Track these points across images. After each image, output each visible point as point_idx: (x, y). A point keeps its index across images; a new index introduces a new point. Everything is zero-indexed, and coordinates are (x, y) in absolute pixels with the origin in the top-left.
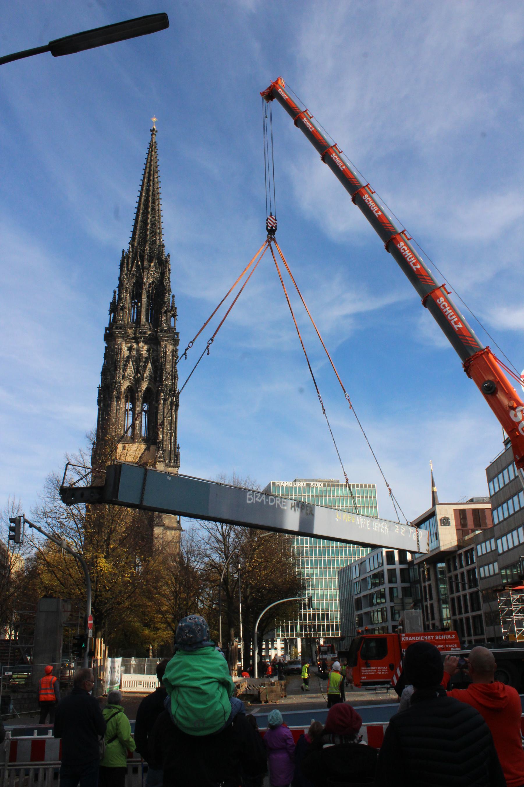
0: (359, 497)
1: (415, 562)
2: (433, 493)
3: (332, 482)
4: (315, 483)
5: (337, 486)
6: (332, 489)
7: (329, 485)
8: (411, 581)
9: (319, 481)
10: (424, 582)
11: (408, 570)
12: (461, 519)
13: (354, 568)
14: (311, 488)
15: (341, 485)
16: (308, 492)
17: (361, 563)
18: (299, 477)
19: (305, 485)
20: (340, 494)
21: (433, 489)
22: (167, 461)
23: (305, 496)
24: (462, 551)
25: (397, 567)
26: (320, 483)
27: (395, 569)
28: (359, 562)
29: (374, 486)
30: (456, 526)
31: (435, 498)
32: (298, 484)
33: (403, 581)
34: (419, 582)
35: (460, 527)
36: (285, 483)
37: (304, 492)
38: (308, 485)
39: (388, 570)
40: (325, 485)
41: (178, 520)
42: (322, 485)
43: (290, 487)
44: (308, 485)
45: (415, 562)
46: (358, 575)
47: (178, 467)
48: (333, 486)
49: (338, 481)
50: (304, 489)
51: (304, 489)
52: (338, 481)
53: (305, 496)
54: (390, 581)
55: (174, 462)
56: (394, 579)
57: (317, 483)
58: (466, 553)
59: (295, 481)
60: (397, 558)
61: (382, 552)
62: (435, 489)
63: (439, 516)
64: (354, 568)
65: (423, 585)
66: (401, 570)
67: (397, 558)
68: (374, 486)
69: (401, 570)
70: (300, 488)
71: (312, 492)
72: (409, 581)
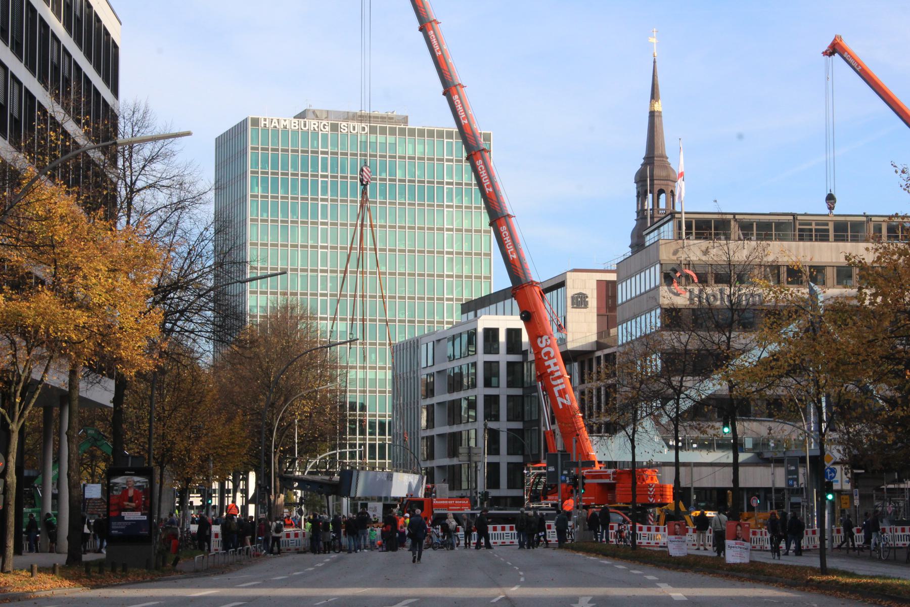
0: (451, 161)
2: (652, 115)
4: (351, 124)
5: (402, 132)
6: (390, 139)
7: (383, 131)
8: (526, 385)
11: (522, 363)
12: (608, 297)
13: (424, 347)
15: (412, 132)
16: (335, 144)
17: (439, 341)
18: (316, 107)
19: (328, 128)
20: (409, 153)
21: (652, 105)
23: (327, 153)
24: (598, 354)
25: (503, 357)
27: (498, 362)
28: (435, 338)
30: (598, 309)
31: (657, 129)
32: (312, 124)
33: (510, 385)
35: (604, 311)
36: (282, 122)
37: (325, 145)
39: (485, 362)
40: (373, 130)
42: (367, 130)
43: (293, 131)
44: (335, 127)
46: (430, 363)
48: (393, 132)
49: (405, 120)
50: (325, 137)
51: (325, 137)
52: (405, 120)
53: (327, 153)
54: (488, 384)
56: (494, 380)
58: (607, 356)
62: (658, 107)
63: (571, 289)
64: (424, 347)
66: (510, 364)
69: (510, 364)
70: (315, 133)
71: (343, 144)
72: (522, 387)
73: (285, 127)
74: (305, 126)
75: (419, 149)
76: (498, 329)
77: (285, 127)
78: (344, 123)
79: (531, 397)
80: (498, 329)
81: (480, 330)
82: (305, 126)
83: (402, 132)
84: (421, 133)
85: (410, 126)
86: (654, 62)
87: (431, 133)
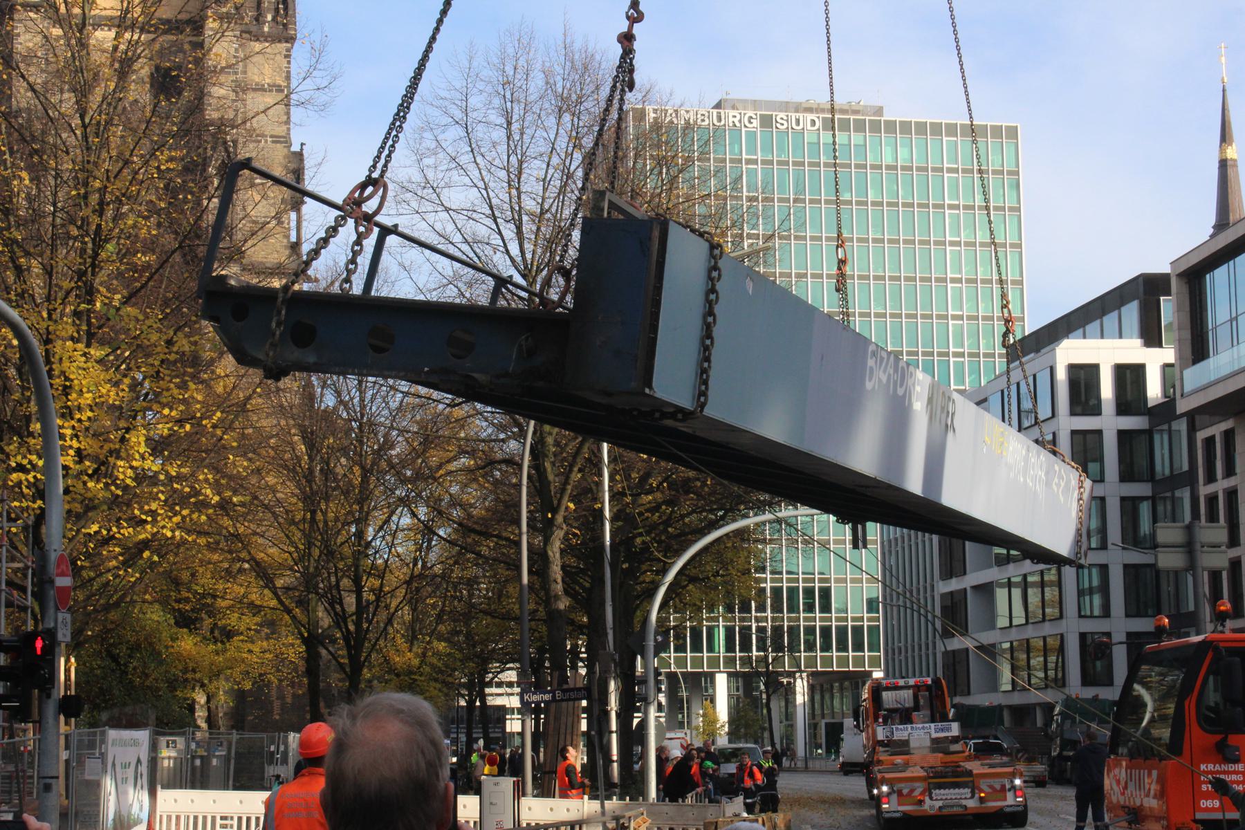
0: (956, 171)
1: (1182, 407)
2: (1224, 164)
3: (856, 112)
4: (794, 116)
5: (875, 127)
6: (856, 138)
8: (1158, 477)
9: (809, 110)
10: (1211, 478)
11: (1149, 433)
14: (779, 132)
15: (890, 126)
16: (768, 148)
18: (734, 95)
19: (756, 123)
20: (888, 159)
21: (1222, 150)
22: (250, 14)
23: (755, 162)
25: (1109, 423)
26: (810, 116)
29: (1013, 132)
33: (1127, 475)
34: (1189, 479)
37: (752, 149)
38: (767, 121)
39: (1073, 432)
41: (293, 239)
42: (818, 124)
44: (767, 121)
45: (1182, 407)
47: (291, 39)
48: (860, 127)
49: (879, 111)
50: (752, 136)
51: (752, 136)
52: (879, 111)
55: (274, 19)
57: (801, 115)
59: (718, 106)
60: (1107, 390)
61: (1052, 370)
62: (1231, 153)
65: (1204, 490)
66: (1123, 435)
67: (1107, 390)
68: (1013, 132)
69: (1123, 435)
70: (736, 130)
72: (1151, 477)
73: (687, 122)
74: (719, 119)
75: (903, 154)
76: (1095, 367)
77: (687, 122)
78: (782, 115)
79: (1173, 499)
80: (1095, 367)
81: (1061, 375)
82: (719, 119)
83: (875, 127)
84: (906, 127)
85: (887, 116)
86: (1224, 91)
87: (921, 128)
